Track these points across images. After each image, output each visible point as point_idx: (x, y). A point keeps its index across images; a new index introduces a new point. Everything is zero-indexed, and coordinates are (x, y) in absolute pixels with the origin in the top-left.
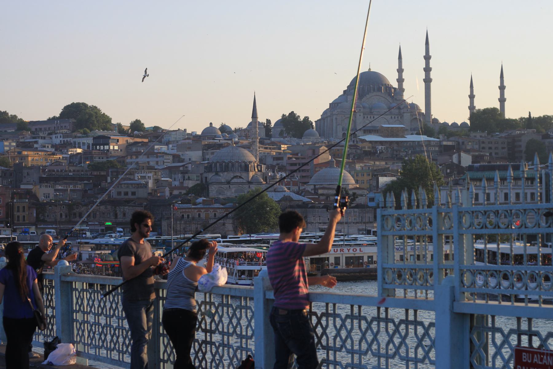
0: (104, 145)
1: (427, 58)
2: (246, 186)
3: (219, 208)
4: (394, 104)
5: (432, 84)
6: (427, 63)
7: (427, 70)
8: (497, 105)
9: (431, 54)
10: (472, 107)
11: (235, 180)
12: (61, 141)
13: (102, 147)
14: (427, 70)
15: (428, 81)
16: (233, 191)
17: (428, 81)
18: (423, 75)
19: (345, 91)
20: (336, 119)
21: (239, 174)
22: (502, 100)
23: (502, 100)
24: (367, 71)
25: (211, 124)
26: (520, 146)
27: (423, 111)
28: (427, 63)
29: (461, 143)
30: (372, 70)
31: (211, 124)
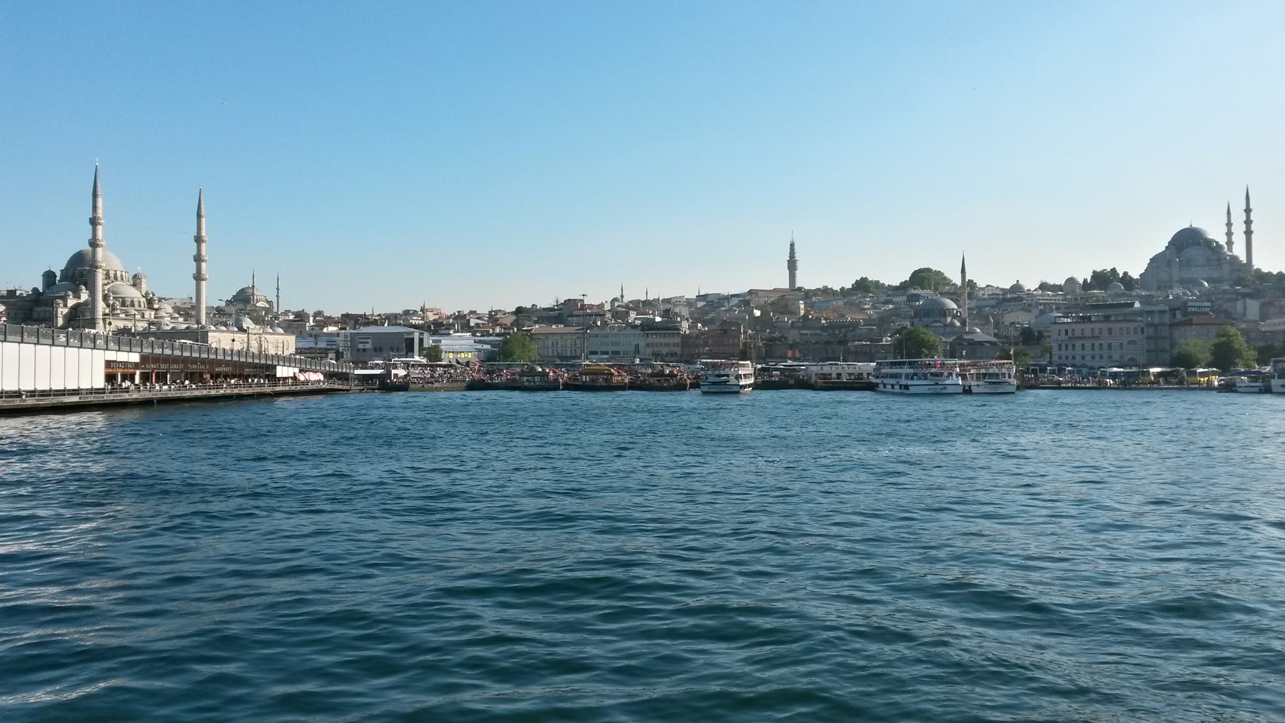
9: (1252, 207)
24: (1188, 226)
25: (1018, 281)
30: (1194, 226)
31: (1018, 281)
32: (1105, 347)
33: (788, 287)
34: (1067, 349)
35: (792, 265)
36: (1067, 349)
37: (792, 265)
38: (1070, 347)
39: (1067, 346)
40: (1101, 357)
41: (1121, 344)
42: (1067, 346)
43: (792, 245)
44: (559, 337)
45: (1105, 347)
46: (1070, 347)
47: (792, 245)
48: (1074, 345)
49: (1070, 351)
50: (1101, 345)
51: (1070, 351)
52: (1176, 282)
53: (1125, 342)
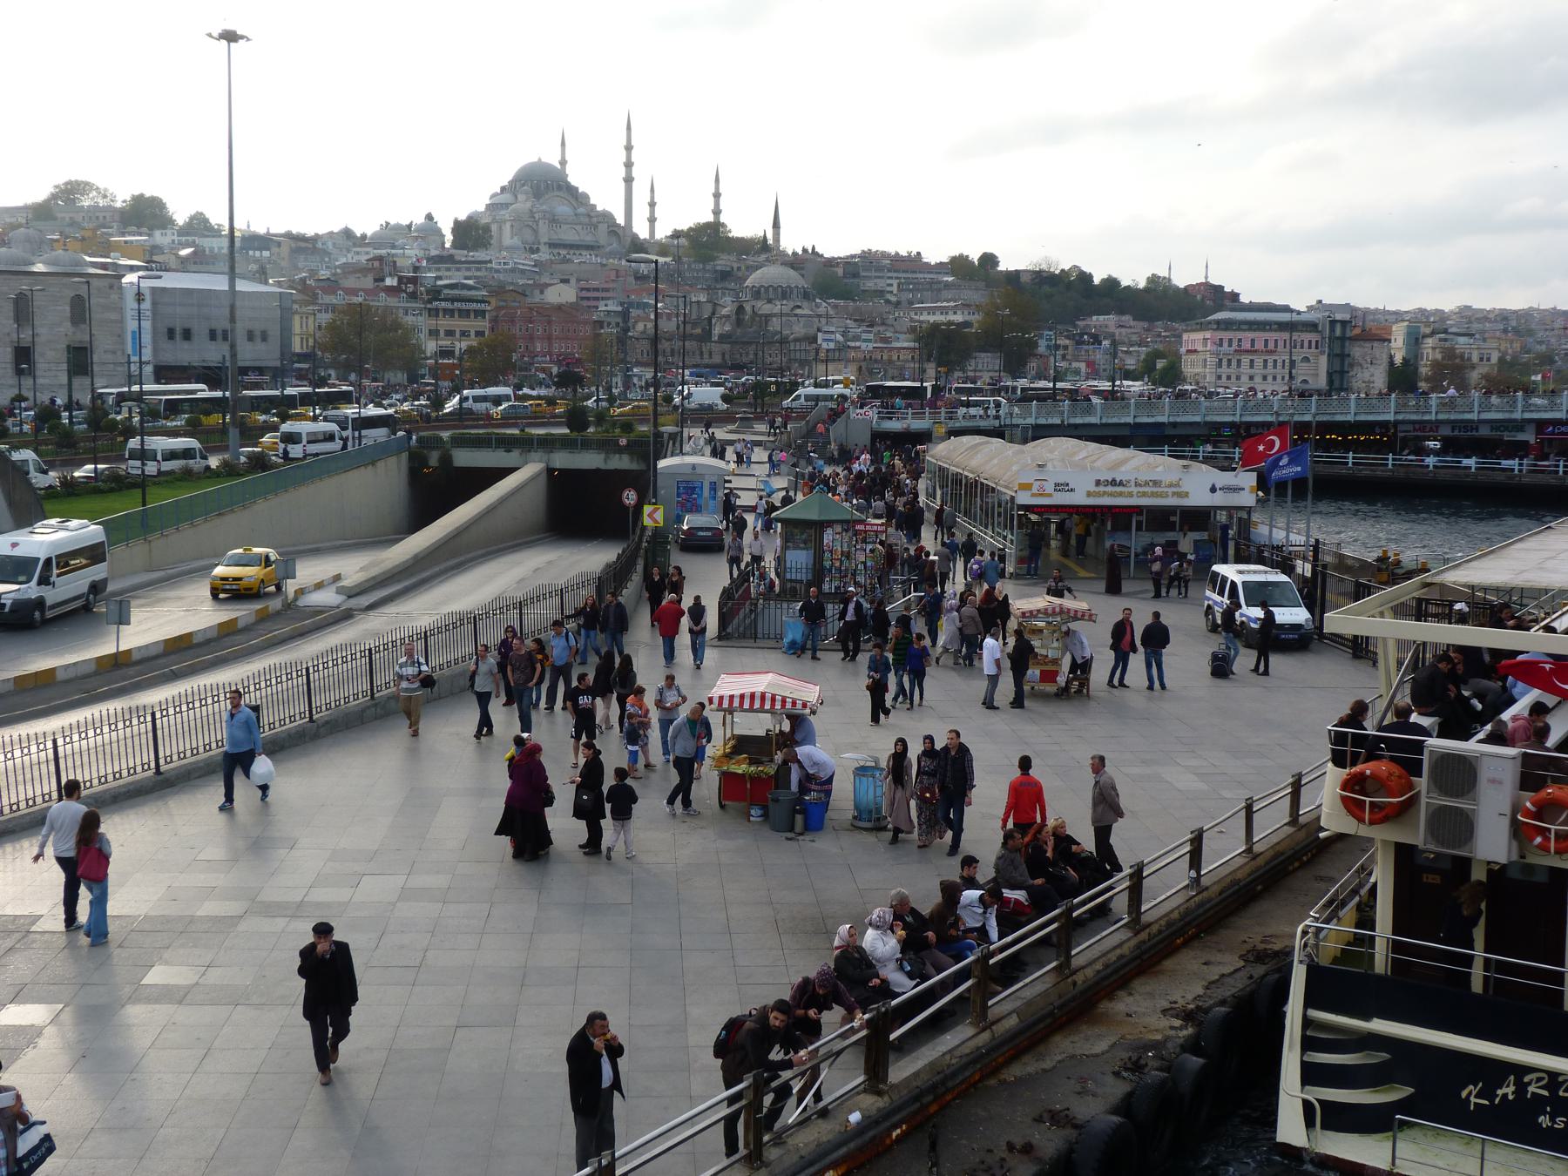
0: (261, 249)
1: (629, 148)
2: (816, 320)
3: (904, 348)
4: (581, 210)
5: (635, 184)
7: (629, 165)
8: (710, 218)
10: (652, 220)
11: (798, 311)
12: (173, 241)
13: (258, 253)
14: (629, 165)
15: (629, 180)
16: (801, 325)
17: (629, 180)
18: (622, 172)
19: (503, 189)
20: (512, 226)
21: (799, 304)
22: (717, 212)
23: (717, 212)
24: (536, 160)
27: (620, 220)
29: (735, 269)
38: (1234, 363)
39: (1229, 361)
40: (1275, 378)
42: (1229, 361)
46: (1234, 363)
48: (1239, 361)
49: (1233, 370)
50: (1275, 361)
51: (1233, 370)
52: (545, 244)
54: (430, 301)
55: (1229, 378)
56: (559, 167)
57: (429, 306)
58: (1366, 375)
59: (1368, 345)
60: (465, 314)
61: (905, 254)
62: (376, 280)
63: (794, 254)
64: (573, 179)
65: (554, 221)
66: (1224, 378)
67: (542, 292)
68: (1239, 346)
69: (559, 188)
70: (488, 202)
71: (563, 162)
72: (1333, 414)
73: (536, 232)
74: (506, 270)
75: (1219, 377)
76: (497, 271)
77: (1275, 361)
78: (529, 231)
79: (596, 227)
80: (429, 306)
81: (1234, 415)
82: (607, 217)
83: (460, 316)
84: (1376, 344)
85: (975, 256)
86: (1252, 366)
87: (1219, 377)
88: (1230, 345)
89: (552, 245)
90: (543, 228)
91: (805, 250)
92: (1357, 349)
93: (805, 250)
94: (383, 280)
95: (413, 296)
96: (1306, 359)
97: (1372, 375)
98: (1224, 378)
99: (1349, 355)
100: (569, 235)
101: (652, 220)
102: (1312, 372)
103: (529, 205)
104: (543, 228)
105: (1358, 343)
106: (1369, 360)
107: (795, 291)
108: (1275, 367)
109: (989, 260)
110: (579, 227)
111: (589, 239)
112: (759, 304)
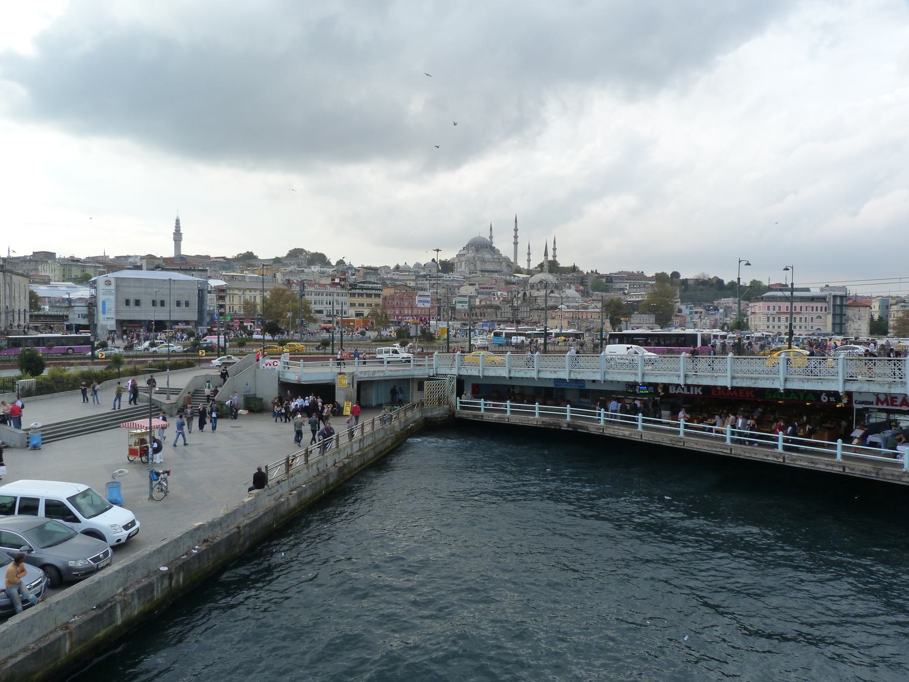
1: (516, 230)
4: (495, 256)
6: (516, 234)
7: (516, 237)
10: (529, 261)
14: (516, 237)
15: (516, 243)
17: (516, 243)
18: (513, 240)
24: (478, 236)
25: (406, 263)
26: (587, 282)
27: (512, 260)
28: (516, 234)
30: (481, 236)
31: (406, 263)
32: (803, 319)
33: (182, 253)
34: (774, 320)
35: (178, 237)
36: (774, 320)
37: (178, 237)
38: (776, 319)
39: (774, 318)
40: (800, 327)
41: (812, 318)
42: (774, 318)
43: (178, 222)
44: (258, 293)
45: (803, 319)
46: (776, 319)
47: (178, 222)
48: (779, 318)
49: (776, 323)
50: (801, 318)
51: (776, 323)
53: (815, 317)
54: (350, 290)
55: (774, 327)
56: (489, 239)
57: (350, 292)
58: (856, 326)
59: (857, 309)
60: (369, 296)
61: (636, 272)
62: (332, 280)
63: (587, 273)
64: (493, 245)
65: (483, 261)
66: (771, 327)
67: (459, 289)
68: (780, 310)
69: (487, 247)
70: (458, 253)
71: (491, 237)
72: (757, 379)
73: (475, 266)
74: (449, 281)
75: (768, 327)
76: (446, 281)
77: (801, 318)
78: (473, 265)
79: (501, 263)
80: (350, 292)
81: (636, 374)
82: (507, 260)
83: (358, 297)
84: (861, 309)
85: (669, 273)
86: (779, 321)
87: (768, 327)
88: (774, 310)
89: (482, 271)
90: (478, 264)
91: (592, 272)
92: (850, 311)
93: (592, 272)
94: (334, 280)
95: (343, 287)
96: (820, 317)
97: (860, 326)
98: (771, 327)
99: (845, 315)
100: (490, 267)
101: (529, 261)
102: (823, 324)
103: (473, 254)
104: (478, 264)
105: (851, 308)
106: (857, 318)
107: (551, 285)
108: (801, 321)
109: (676, 275)
110: (494, 264)
111: (498, 268)
112: (533, 291)
